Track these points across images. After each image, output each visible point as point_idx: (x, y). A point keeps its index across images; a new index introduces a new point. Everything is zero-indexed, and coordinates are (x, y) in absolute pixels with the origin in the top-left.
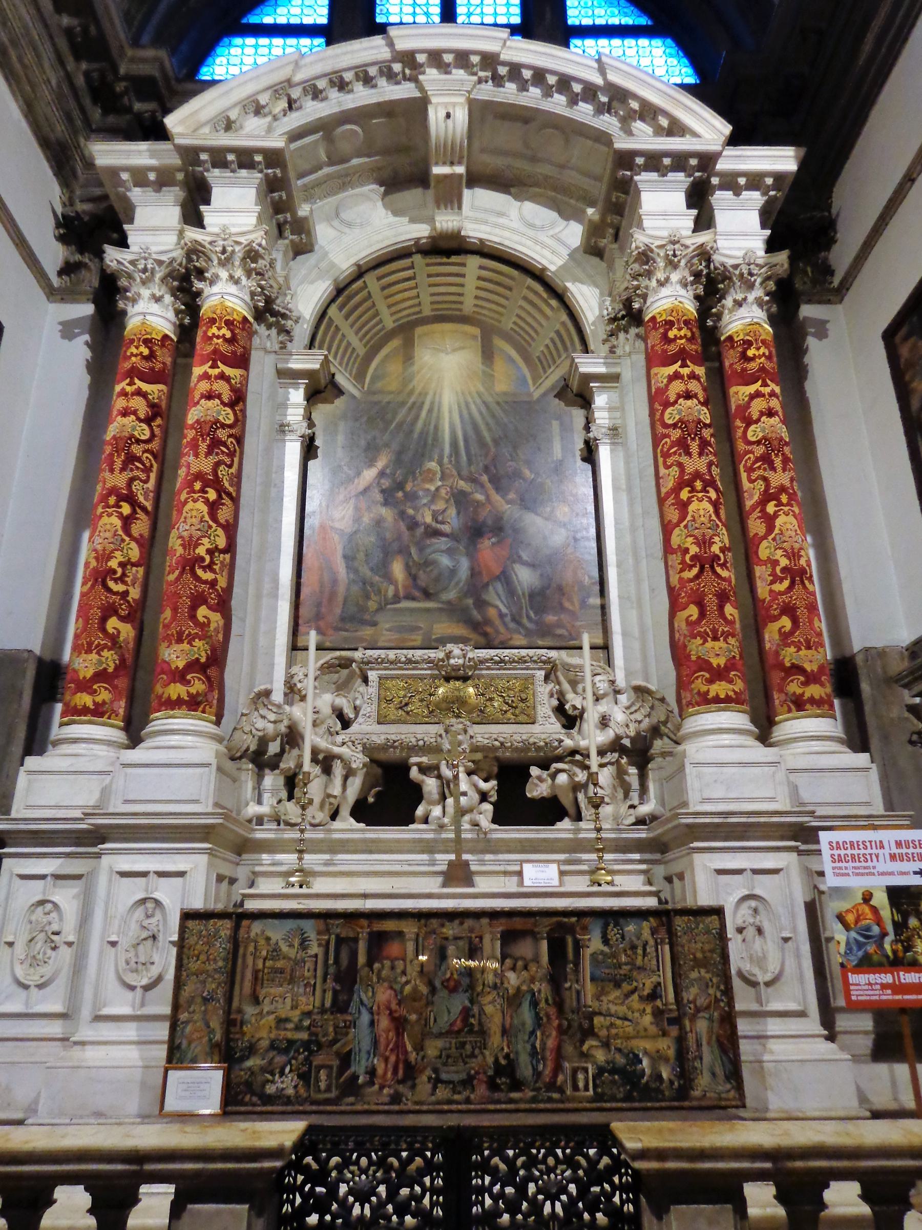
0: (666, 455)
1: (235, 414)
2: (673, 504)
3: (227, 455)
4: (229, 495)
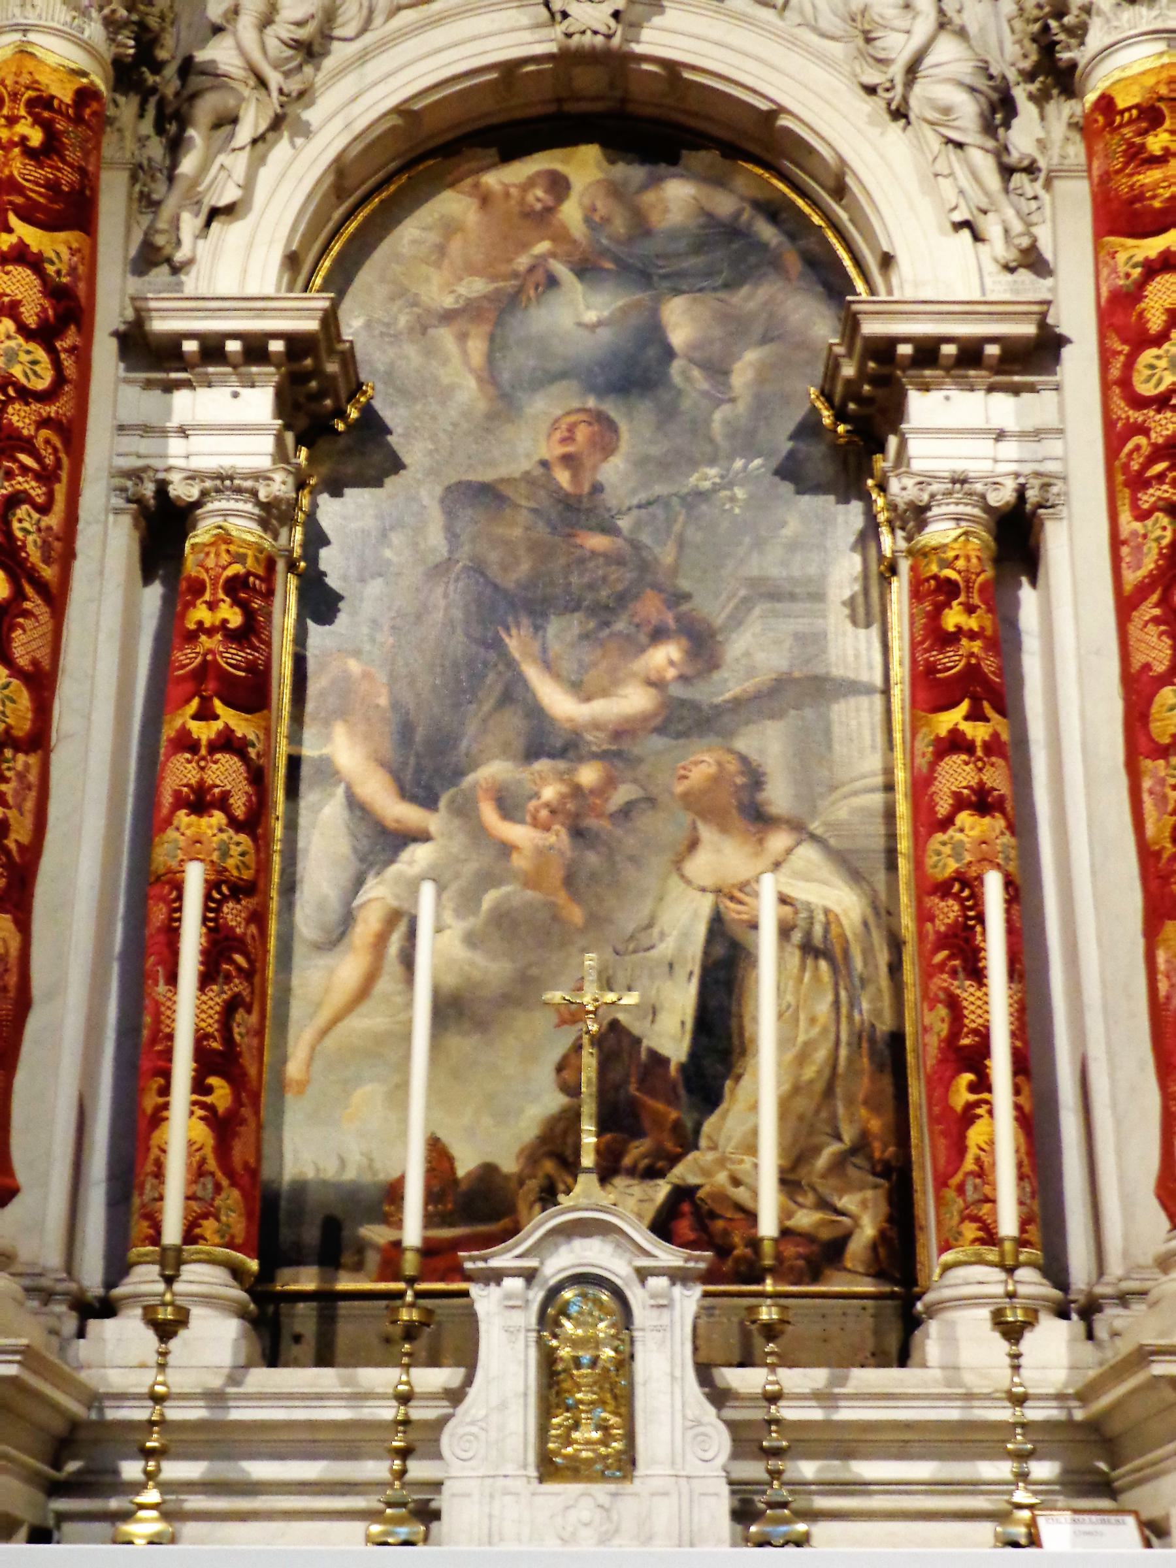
0: (1139, 483)
1: (57, 364)
2: (1156, 620)
3: (38, 477)
4: (42, 587)
